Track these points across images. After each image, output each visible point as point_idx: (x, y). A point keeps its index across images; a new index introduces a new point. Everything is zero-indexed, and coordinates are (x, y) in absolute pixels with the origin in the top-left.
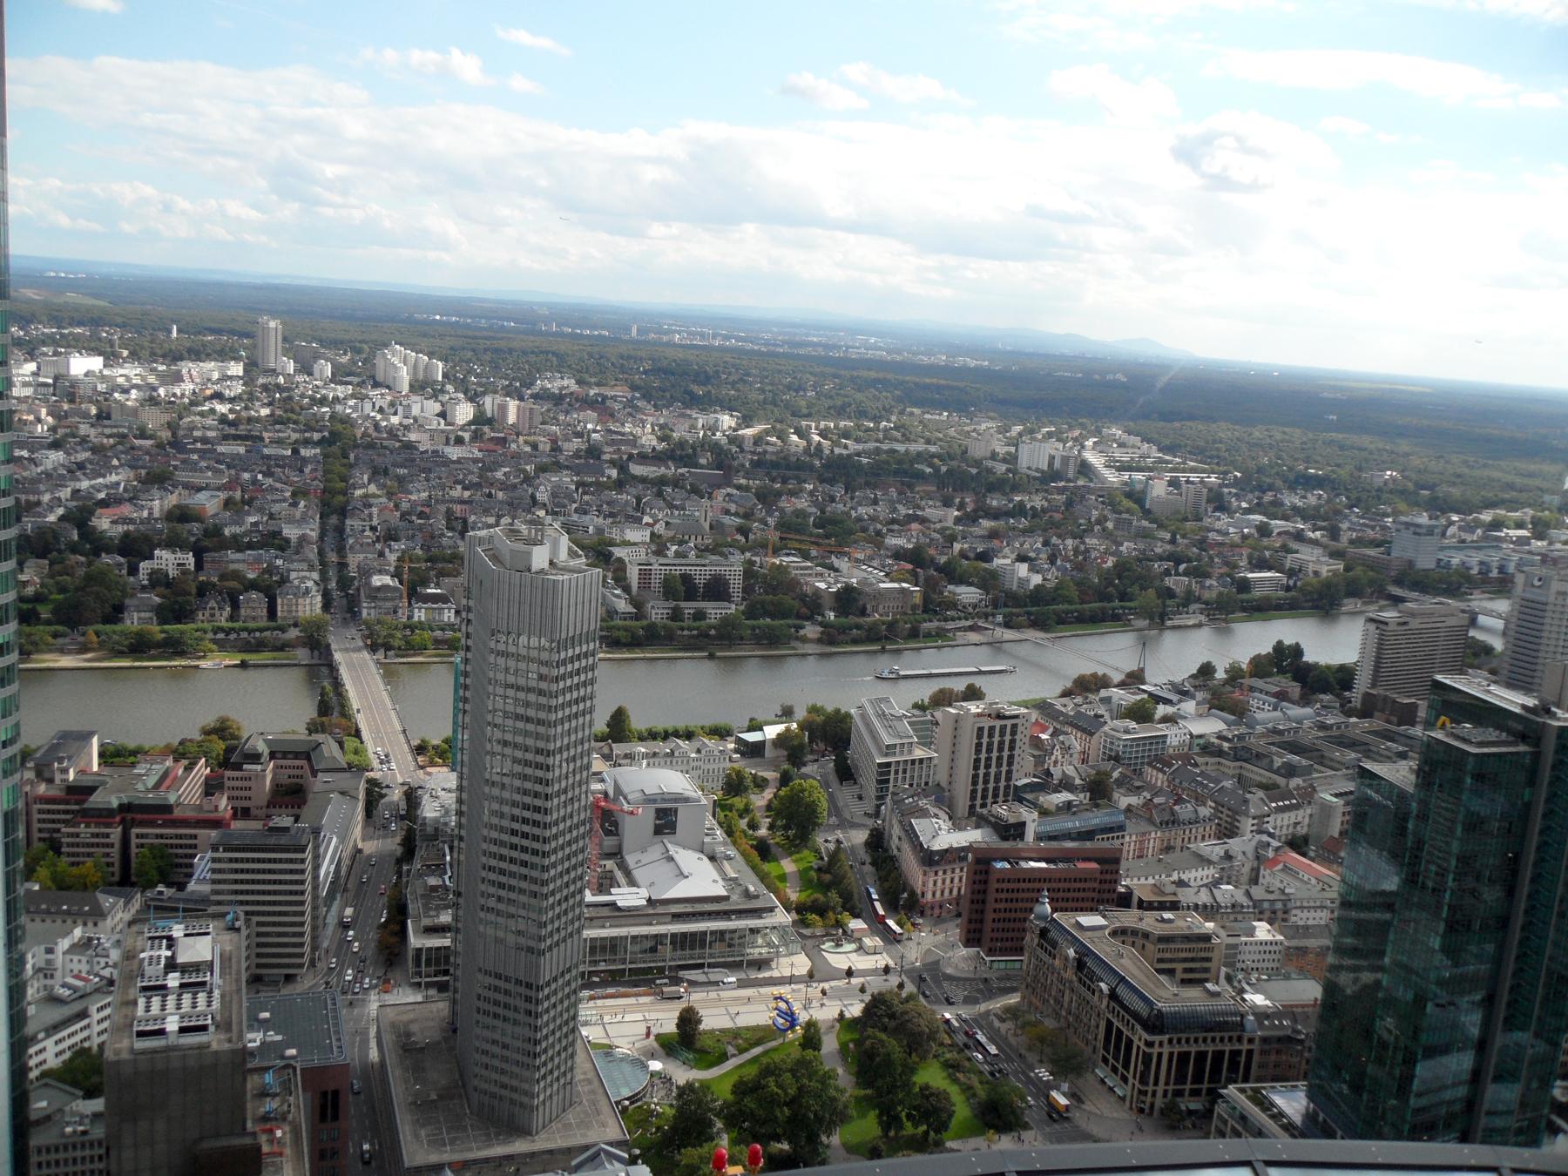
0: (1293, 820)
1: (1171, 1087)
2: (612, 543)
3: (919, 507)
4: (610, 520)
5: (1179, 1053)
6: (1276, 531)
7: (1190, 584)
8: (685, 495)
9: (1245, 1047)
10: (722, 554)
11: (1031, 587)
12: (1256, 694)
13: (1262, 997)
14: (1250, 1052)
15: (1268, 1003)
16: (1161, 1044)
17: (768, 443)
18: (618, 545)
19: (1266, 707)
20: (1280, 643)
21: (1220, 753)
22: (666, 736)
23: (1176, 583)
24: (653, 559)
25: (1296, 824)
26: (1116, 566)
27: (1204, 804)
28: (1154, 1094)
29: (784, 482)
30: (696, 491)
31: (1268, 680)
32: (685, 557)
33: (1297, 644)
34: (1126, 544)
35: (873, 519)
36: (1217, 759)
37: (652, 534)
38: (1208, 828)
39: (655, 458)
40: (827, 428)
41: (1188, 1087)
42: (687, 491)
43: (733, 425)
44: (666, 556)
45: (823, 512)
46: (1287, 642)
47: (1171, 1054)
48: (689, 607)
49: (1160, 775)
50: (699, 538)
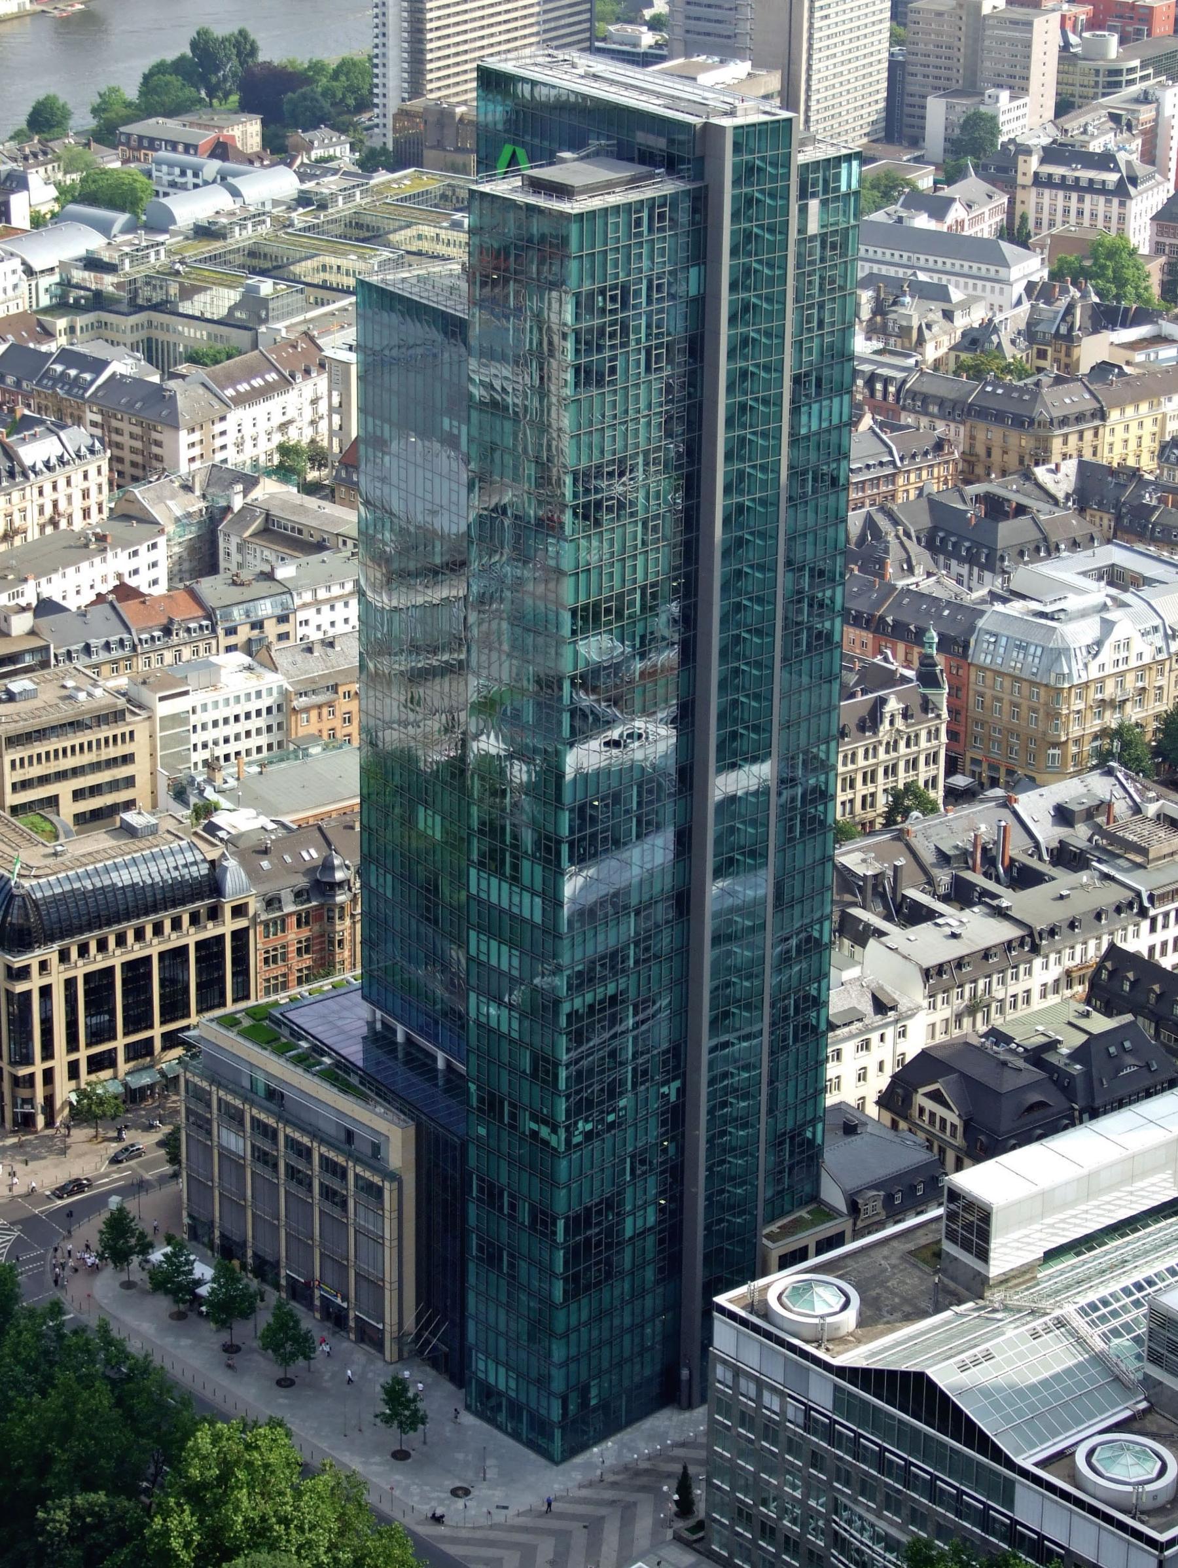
0: (278, 419)
1: (83, 1054)
5: (88, 977)
9: (228, 926)
12: (163, 154)
13: (252, 812)
14: (240, 936)
15: (265, 821)
16: (43, 966)
19: (190, 178)
20: (203, 34)
25: (283, 427)
27: (78, 421)
28: (48, 1075)
33: (243, 33)
41: (120, 1043)
46: (221, 31)
47: (70, 984)
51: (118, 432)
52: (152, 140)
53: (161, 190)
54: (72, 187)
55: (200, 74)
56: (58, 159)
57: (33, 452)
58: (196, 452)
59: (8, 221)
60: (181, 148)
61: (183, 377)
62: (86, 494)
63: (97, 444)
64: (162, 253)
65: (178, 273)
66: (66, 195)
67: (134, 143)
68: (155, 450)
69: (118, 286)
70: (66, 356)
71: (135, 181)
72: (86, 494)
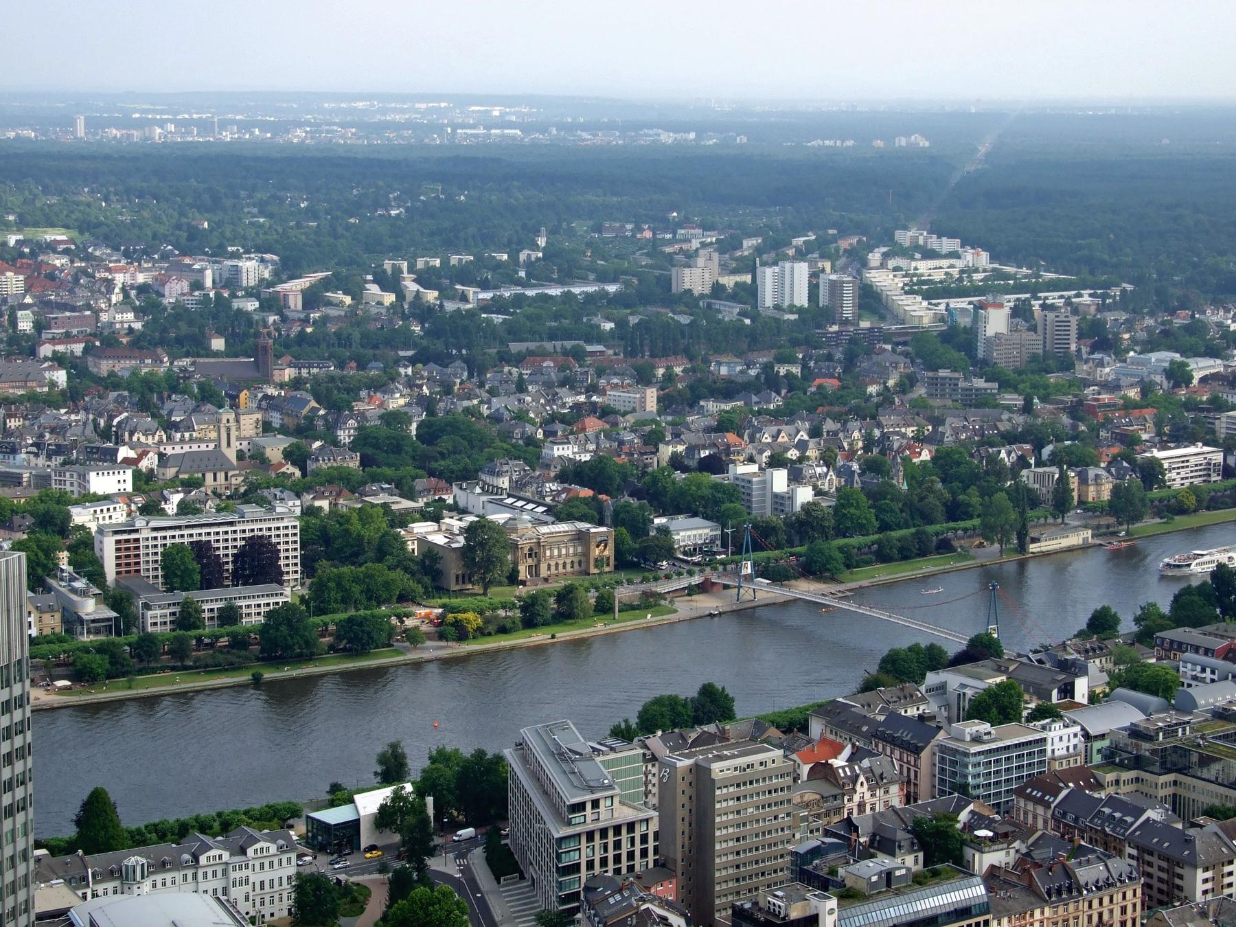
2: (64, 500)
3: (593, 389)
4: (60, 459)
6: (1197, 376)
7: (1063, 478)
8: (191, 403)
10: (261, 502)
11: (798, 508)
12: (1189, 655)
17: (329, 303)
18: (76, 503)
19: (1208, 675)
21: (1138, 762)
22: (182, 831)
23: (1038, 478)
24: (140, 522)
26: (934, 459)
27: (1120, 853)
29: (362, 366)
30: (208, 396)
31: (1208, 628)
32: (197, 511)
34: (949, 420)
35: (521, 416)
36: (1133, 774)
37: (137, 476)
38: (1129, 894)
39: (140, 344)
40: (430, 270)
42: (192, 396)
43: (267, 275)
44: (162, 513)
45: (431, 412)
48: (210, 603)
49: (1040, 810)
50: (221, 476)
51: (1150, 864)
52: (1180, 644)
53: (1186, 682)
54: (1120, 675)
55: (1217, 597)
56: (1111, 653)
57: (1088, 873)
58: (1209, 886)
59: (1073, 697)
60: (1201, 651)
61: (1201, 826)
62: (1124, 910)
63: (1134, 873)
64: (1188, 728)
65: (1199, 745)
66: (1116, 681)
67: (1166, 645)
68: (1178, 881)
69: (1154, 752)
70: (1112, 801)
71: (1167, 673)
72: (1124, 910)
